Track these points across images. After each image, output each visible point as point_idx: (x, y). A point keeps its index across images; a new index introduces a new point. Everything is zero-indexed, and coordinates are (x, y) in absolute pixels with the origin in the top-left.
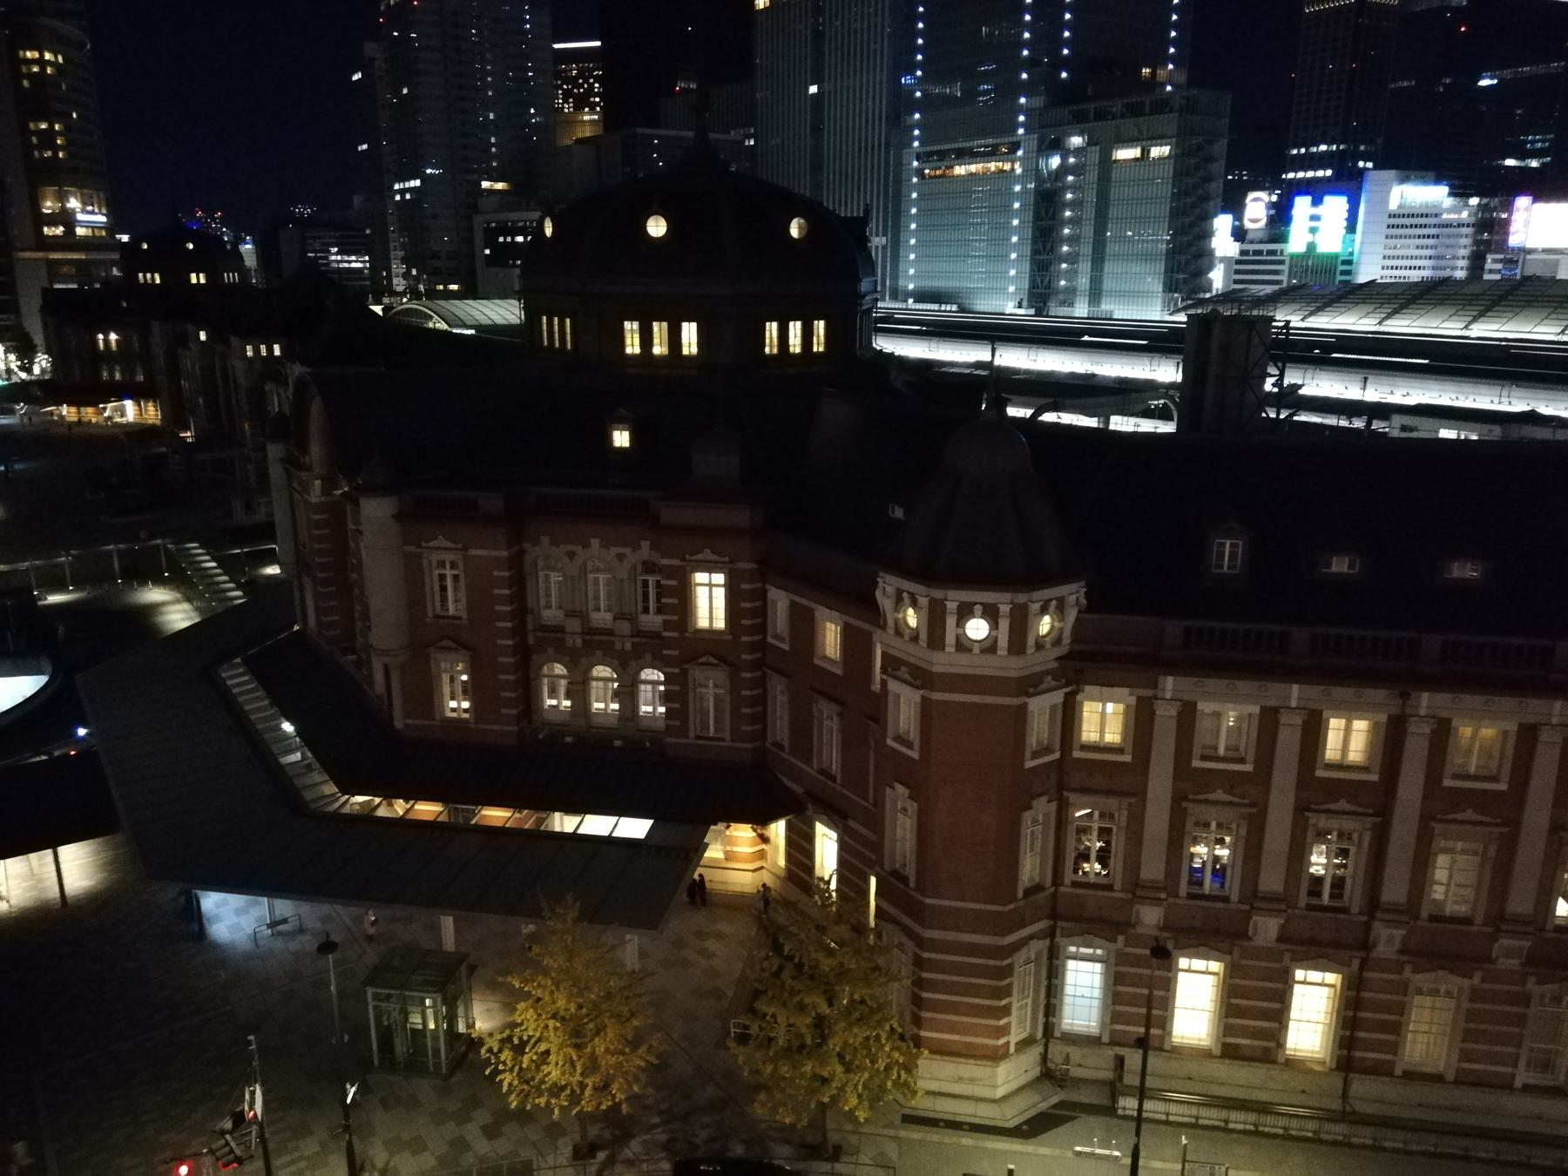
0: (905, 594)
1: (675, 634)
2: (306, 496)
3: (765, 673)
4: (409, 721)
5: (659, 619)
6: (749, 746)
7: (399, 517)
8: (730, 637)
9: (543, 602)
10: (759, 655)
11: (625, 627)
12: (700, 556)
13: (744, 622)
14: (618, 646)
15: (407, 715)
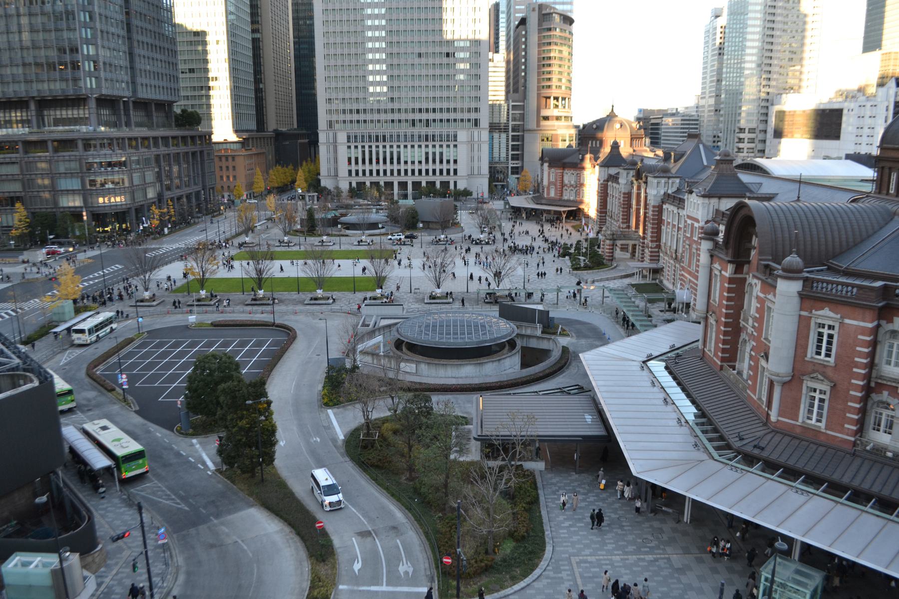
2: (723, 272)
4: (780, 419)
7: (799, 293)
9: (884, 361)
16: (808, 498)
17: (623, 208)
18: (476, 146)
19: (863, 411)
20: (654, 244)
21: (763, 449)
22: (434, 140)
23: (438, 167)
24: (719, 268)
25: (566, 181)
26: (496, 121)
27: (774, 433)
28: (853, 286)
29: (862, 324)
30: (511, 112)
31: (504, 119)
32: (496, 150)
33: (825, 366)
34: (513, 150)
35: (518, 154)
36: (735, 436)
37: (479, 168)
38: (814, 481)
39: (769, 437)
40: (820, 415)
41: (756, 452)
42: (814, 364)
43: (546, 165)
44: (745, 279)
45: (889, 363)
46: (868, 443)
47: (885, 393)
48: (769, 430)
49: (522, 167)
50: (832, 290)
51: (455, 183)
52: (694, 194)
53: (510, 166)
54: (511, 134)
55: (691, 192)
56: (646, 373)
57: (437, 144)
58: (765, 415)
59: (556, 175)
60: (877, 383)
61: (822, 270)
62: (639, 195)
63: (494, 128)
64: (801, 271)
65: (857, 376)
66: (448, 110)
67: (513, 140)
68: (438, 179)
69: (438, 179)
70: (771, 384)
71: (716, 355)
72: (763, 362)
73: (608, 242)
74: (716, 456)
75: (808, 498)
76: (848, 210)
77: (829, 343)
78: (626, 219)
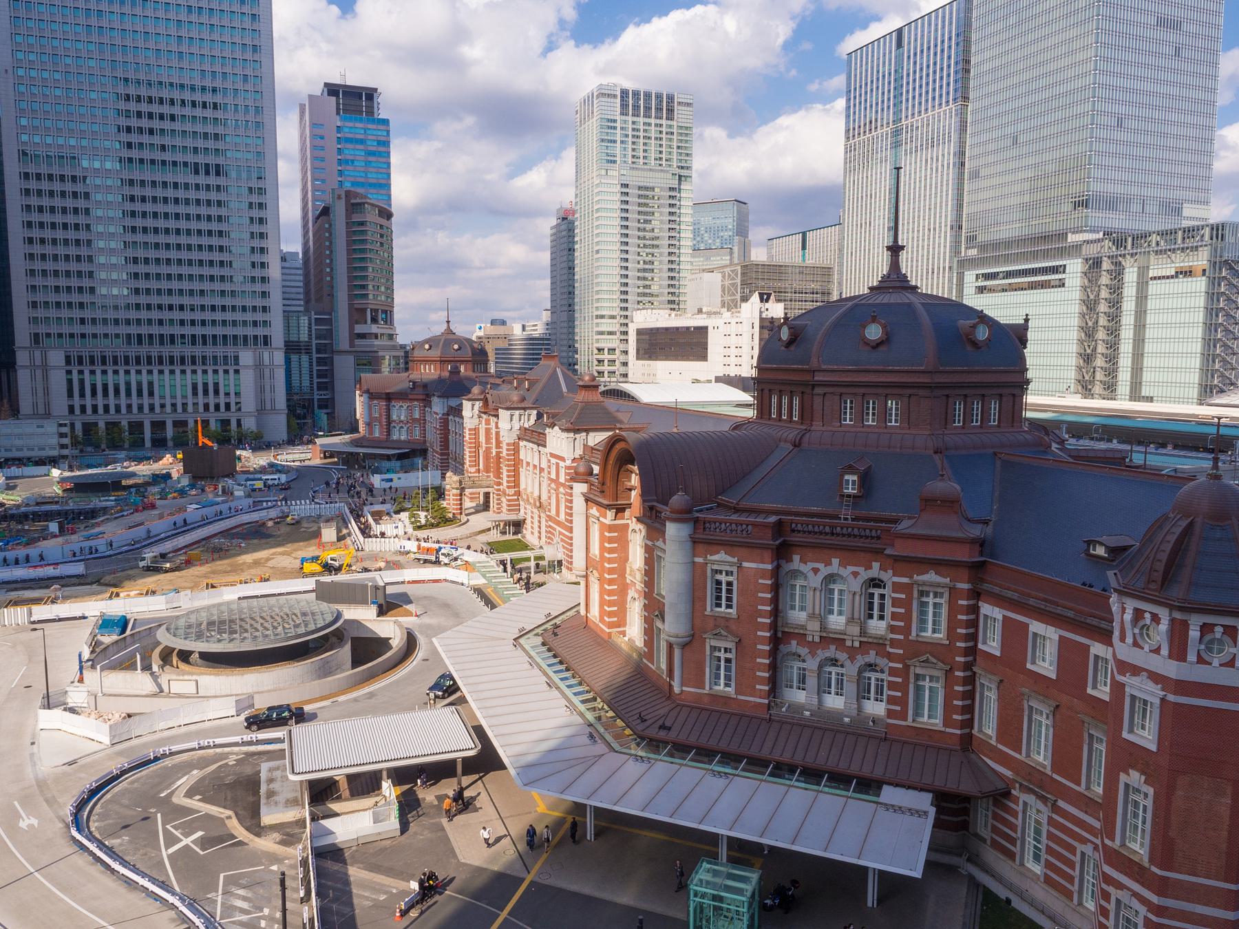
0: (1147, 616)
1: (901, 637)
2: (601, 519)
3: (975, 673)
4: (684, 689)
5: (883, 624)
6: (958, 732)
8: (948, 642)
10: (970, 658)
11: (855, 630)
12: (925, 577)
13: (959, 631)
14: (849, 643)
15: (682, 684)
16: (728, 781)
18: (267, 372)
19: (774, 668)
20: (512, 491)
21: (669, 729)
22: (204, 364)
24: (597, 514)
25: (394, 417)
26: (294, 338)
27: (679, 707)
29: (762, 566)
30: (314, 327)
31: (304, 337)
32: (295, 377)
33: (728, 619)
34: (319, 376)
35: (326, 383)
36: (635, 717)
37: (273, 401)
38: (731, 758)
39: (674, 713)
40: (728, 678)
41: (662, 734)
42: (715, 618)
44: (627, 525)
45: (793, 608)
46: (782, 705)
47: (794, 643)
48: (674, 705)
49: (333, 399)
51: (239, 422)
52: (556, 428)
54: (315, 356)
55: (552, 426)
56: (520, 652)
58: (667, 688)
59: (380, 409)
60: (783, 632)
61: (711, 508)
63: (292, 348)
65: (762, 627)
67: (319, 364)
70: (670, 647)
71: (602, 620)
72: (659, 624)
73: (455, 491)
74: (616, 746)
75: (728, 781)
77: (729, 591)
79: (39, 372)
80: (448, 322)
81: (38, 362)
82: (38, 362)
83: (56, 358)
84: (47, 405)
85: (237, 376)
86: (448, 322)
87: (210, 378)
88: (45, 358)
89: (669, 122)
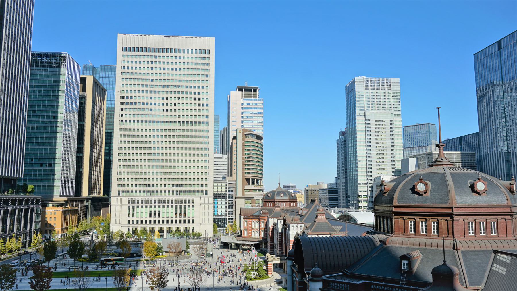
17: (279, 242)
18: (206, 206)
23: (157, 219)
28: (347, 283)
31: (224, 192)
34: (229, 208)
37: (208, 219)
43: (242, 217)
50: (335, 286)
53: (228, 218)
54: (228, 199)
57: (157, 205)
61: (340, 275)
62: (285, 234)
63: (217, 196)
64: (321, 276)
66: (177, 186)
68: (182, 227)
69: (182, 227)
76: (328, 240)
78: (281, 248)
79: (119, 207)
80: (279, 184)
81: (119, 203)
82: (119, 203)
83: (125, 201)
84: (121, 220)
85: (193, 208)
86: (279, 184)
87: (157, 209)
88: (121, 201)
89: (389, 91)
